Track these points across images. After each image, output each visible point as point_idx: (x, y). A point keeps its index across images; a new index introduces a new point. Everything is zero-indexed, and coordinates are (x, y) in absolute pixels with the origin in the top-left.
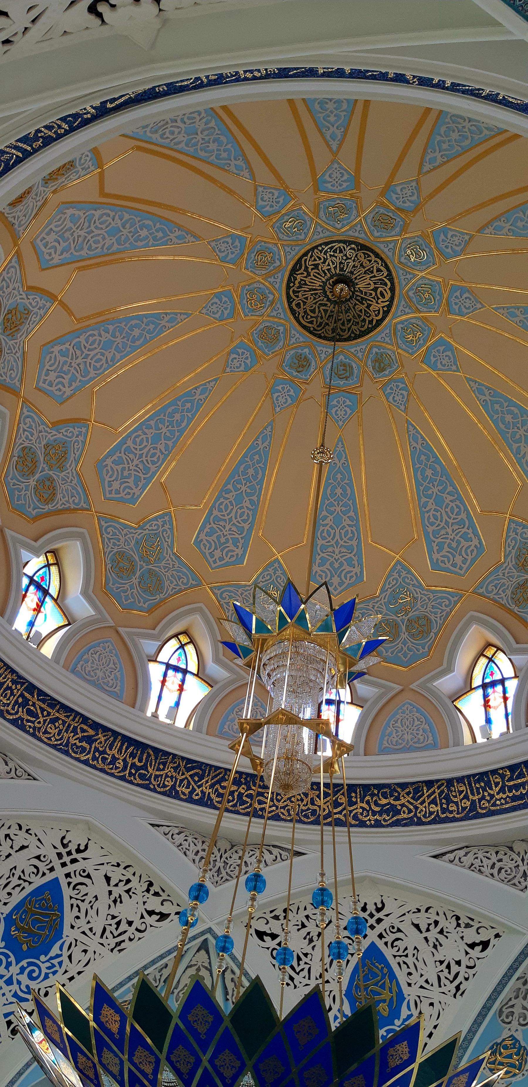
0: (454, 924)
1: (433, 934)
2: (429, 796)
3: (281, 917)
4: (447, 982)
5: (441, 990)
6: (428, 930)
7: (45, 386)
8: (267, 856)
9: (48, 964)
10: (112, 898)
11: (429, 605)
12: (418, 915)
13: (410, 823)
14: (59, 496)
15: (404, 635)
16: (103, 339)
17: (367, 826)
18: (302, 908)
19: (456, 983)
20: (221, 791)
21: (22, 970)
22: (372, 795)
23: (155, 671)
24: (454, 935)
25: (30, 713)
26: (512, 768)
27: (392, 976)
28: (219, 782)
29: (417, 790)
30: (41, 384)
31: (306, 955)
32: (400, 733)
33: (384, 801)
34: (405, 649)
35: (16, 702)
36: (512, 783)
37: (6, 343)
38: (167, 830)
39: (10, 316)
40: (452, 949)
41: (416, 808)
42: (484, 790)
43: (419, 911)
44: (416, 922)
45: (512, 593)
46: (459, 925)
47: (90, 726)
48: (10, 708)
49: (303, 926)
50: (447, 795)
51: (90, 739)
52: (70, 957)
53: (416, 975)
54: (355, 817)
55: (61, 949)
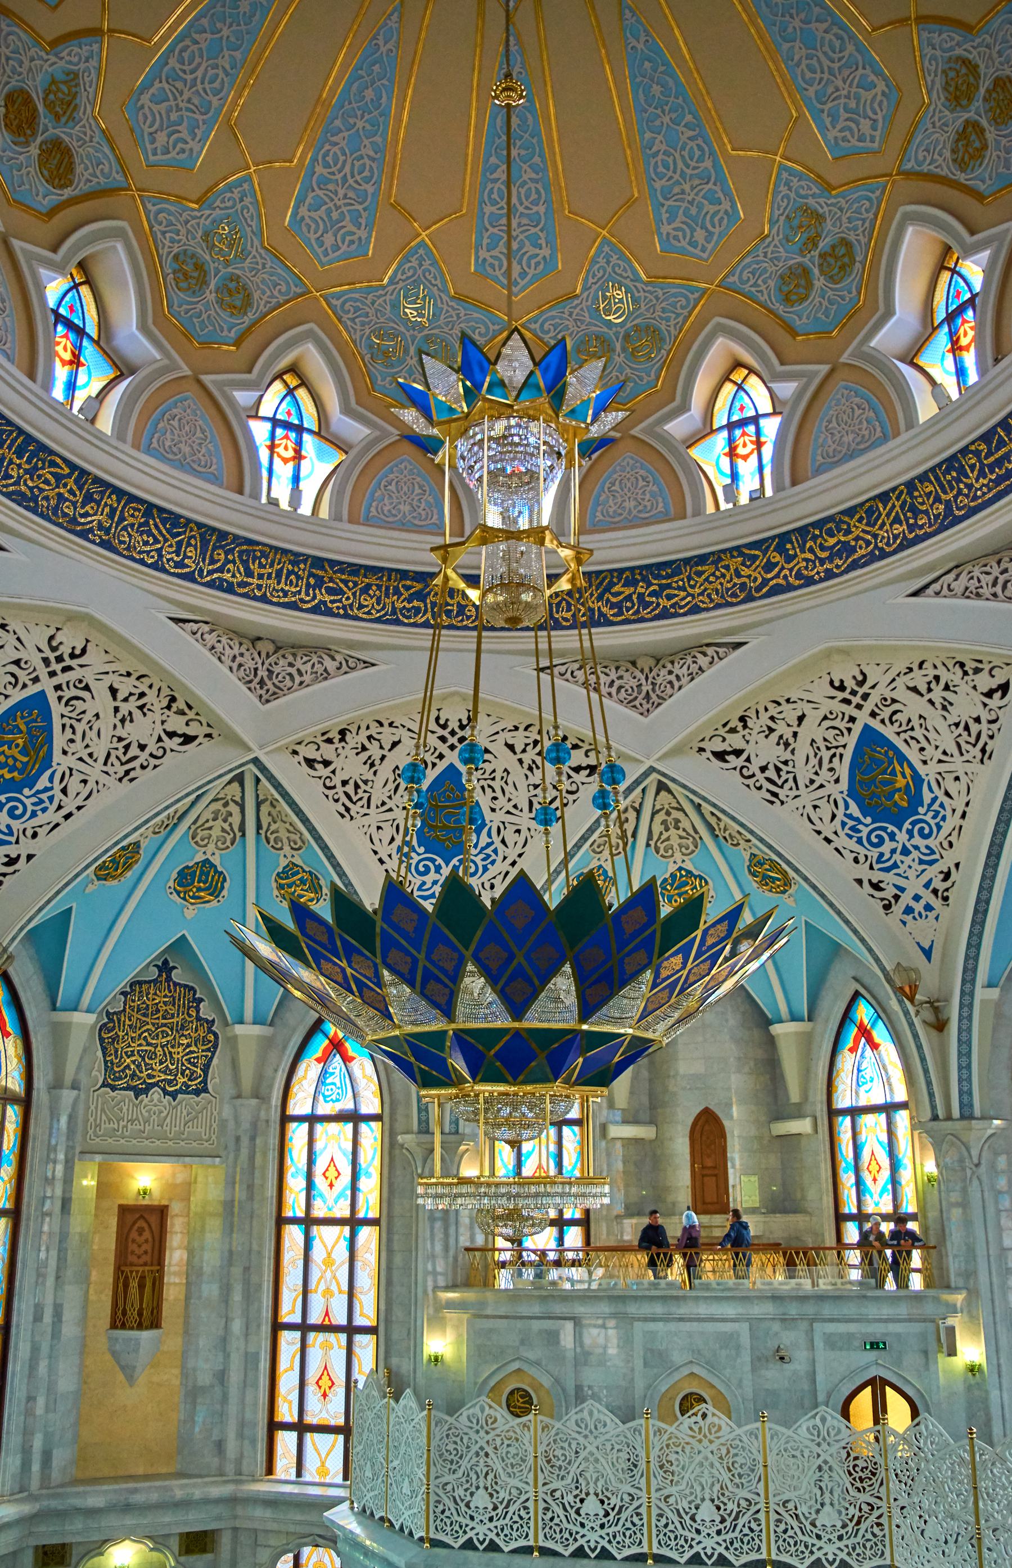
1: (938, 694)
2: (888, 515)
3: (740, 728)
4: (969, 747)
5: (965, 758)
6: (930, 690)
7: (159, 157)
8: (703, 661)
10: (526, 765)
11: (844, 219)
12: (911, 675)
13: (871, 559)
14: (256, 296)
15: (819, 282)
16: (204, 46)
17: (815, 583)
18: (762, 710)
19: (980, 745)
20: (614, 600)
22: (814, 538)
24: (964, 688)
25: (330, 591)
26: (986, 438)
27: (902, 758)
28: (607, 589)
29: (870, 512)
30: (152, 158)
31: (786, 763)
32: (837, 436)
33: (832, 541)
34: (825, 303)
35: (308, 585)
36: (992, 459)
37: (70, 135)
38: (563, 669)
39: (52, 97)
40: (967, 704)
41: (875, 536)
42: (958, 481)
43: (911, 670)
44: (911, 685)
45: (953, 151)
46: (966, 673)
47: (413, 579)
48: (303, 595)
49: (771, 730)
50: (912, 505)
51: (421, 596)
52: (503, 842)
53: (930, 750)
54: (799, 576)
55: (489, 835)
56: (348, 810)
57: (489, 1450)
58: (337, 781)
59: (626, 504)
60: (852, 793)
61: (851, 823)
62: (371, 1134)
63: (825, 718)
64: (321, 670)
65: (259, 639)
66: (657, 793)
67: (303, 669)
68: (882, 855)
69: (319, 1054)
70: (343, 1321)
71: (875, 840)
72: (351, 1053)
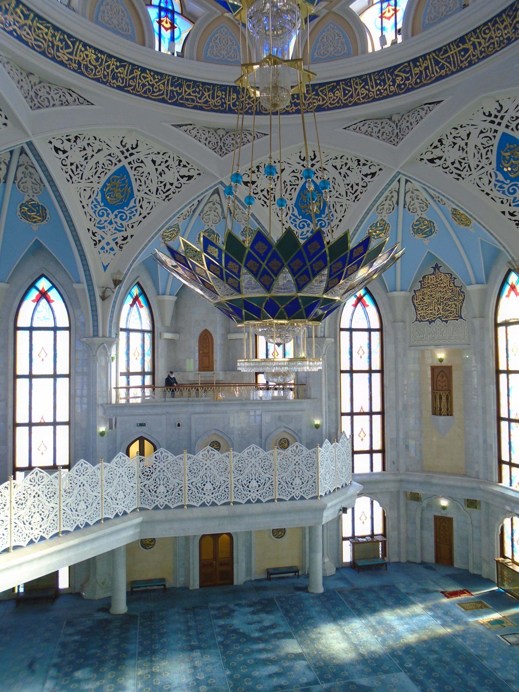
0: (356, 163)
1: (344, 170)
6: (341, 168)
9: (129, 211)
21: (116, 216)
23: (153, 13)
43: (337, 158)
46: (359, 164)
56: (71, 178)
57: (165, 469)
58: (68, 162)
59: (222, 52)
60: (296, 205)
61: (293, 218)
62: (64, 337)
63: (293, 172)
64: (64, 100)
65: (32, 74)
66: (213, 194)
67: (55, 97)
68: (303, 232)
69: (34, 298)
70: (51, 420)
71: (301, 226)
72: (52, 298)
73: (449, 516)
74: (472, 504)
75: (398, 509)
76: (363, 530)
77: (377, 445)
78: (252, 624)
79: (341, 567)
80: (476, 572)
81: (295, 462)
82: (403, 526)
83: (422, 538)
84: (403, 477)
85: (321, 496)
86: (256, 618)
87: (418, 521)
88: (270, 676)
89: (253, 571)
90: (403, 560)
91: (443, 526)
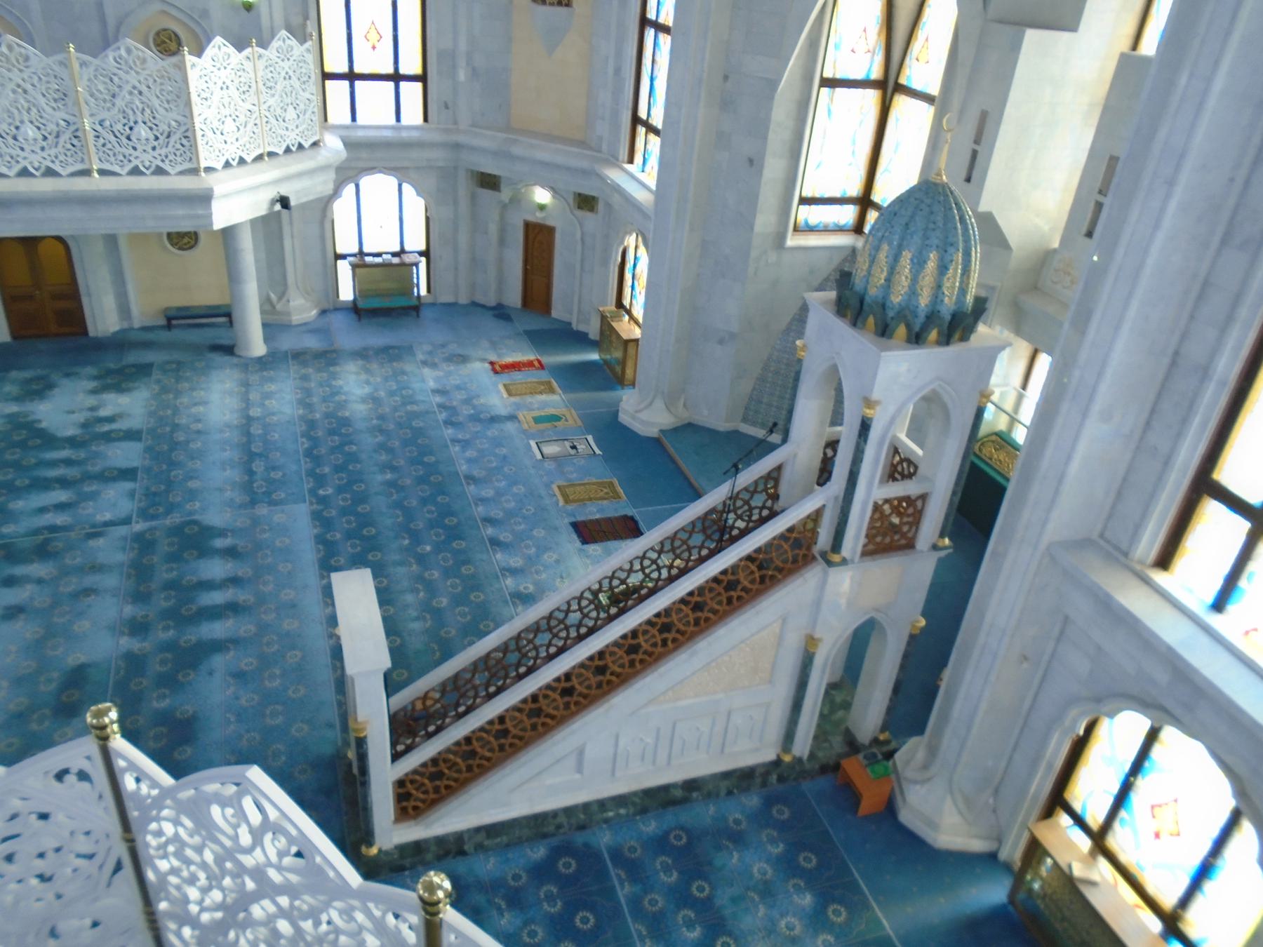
73: (550, 223)
74: (586, 202)
75: (456, 203)
76: (381, 241)
77: (411, 63)
78: (73, 412)
79: (331, 307)
80: (582, 328)
81: (129, 87)
82: (463, 239)
83: (500, 261)
84: (461, 139)
85: (209, 170)
86: (91, 401)
87: (493, 228)
88: (43, 510)
89: (135, 310)
90: (463, 300)
91: (538, 239)
